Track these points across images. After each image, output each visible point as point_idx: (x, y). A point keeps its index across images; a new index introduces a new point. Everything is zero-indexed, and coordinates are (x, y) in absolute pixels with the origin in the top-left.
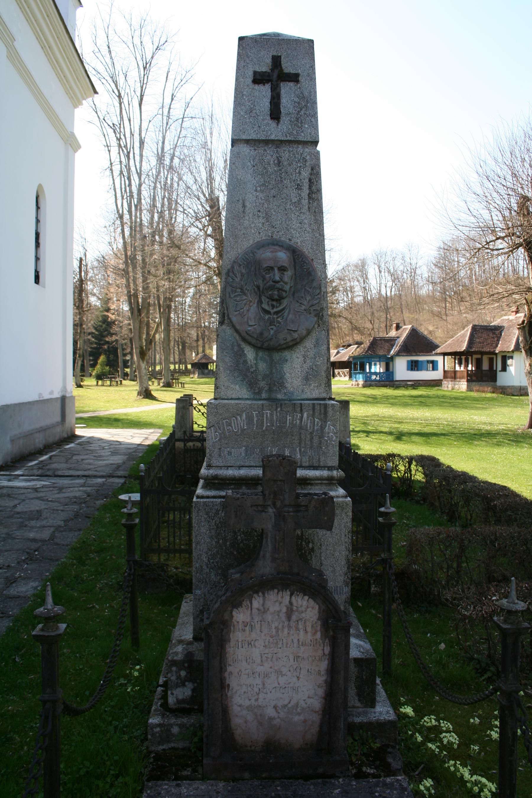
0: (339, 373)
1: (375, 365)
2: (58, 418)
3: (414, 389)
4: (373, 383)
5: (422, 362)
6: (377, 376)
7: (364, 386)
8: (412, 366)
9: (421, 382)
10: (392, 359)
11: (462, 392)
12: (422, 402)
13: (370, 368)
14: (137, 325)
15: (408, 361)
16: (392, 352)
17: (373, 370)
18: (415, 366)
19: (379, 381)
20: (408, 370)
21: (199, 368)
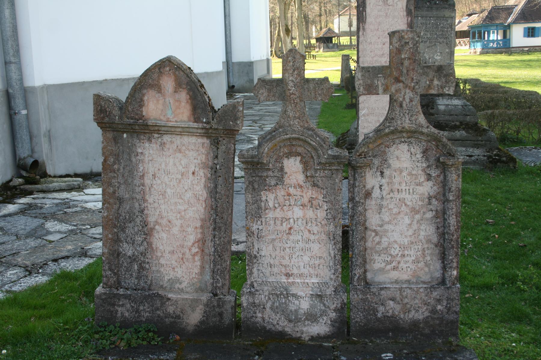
0: (460, 42)
1: (493, 33)
2: (266, 72)
3: (528, 54)
4: (490, 50)
5: (539, 28)
6: (493, 44)
7: (482, 53)
8: (529, 32)
9: (537, 48)
10: (509, 26)
12: (528, 64)
13: (489, 36)
14: (283, 7)
15: (525, 28)
16: (509, 20)
17: (491, 38)
18: (532, 32)
19: (496, 48)
20: (524, 36)
21: (324, 43)
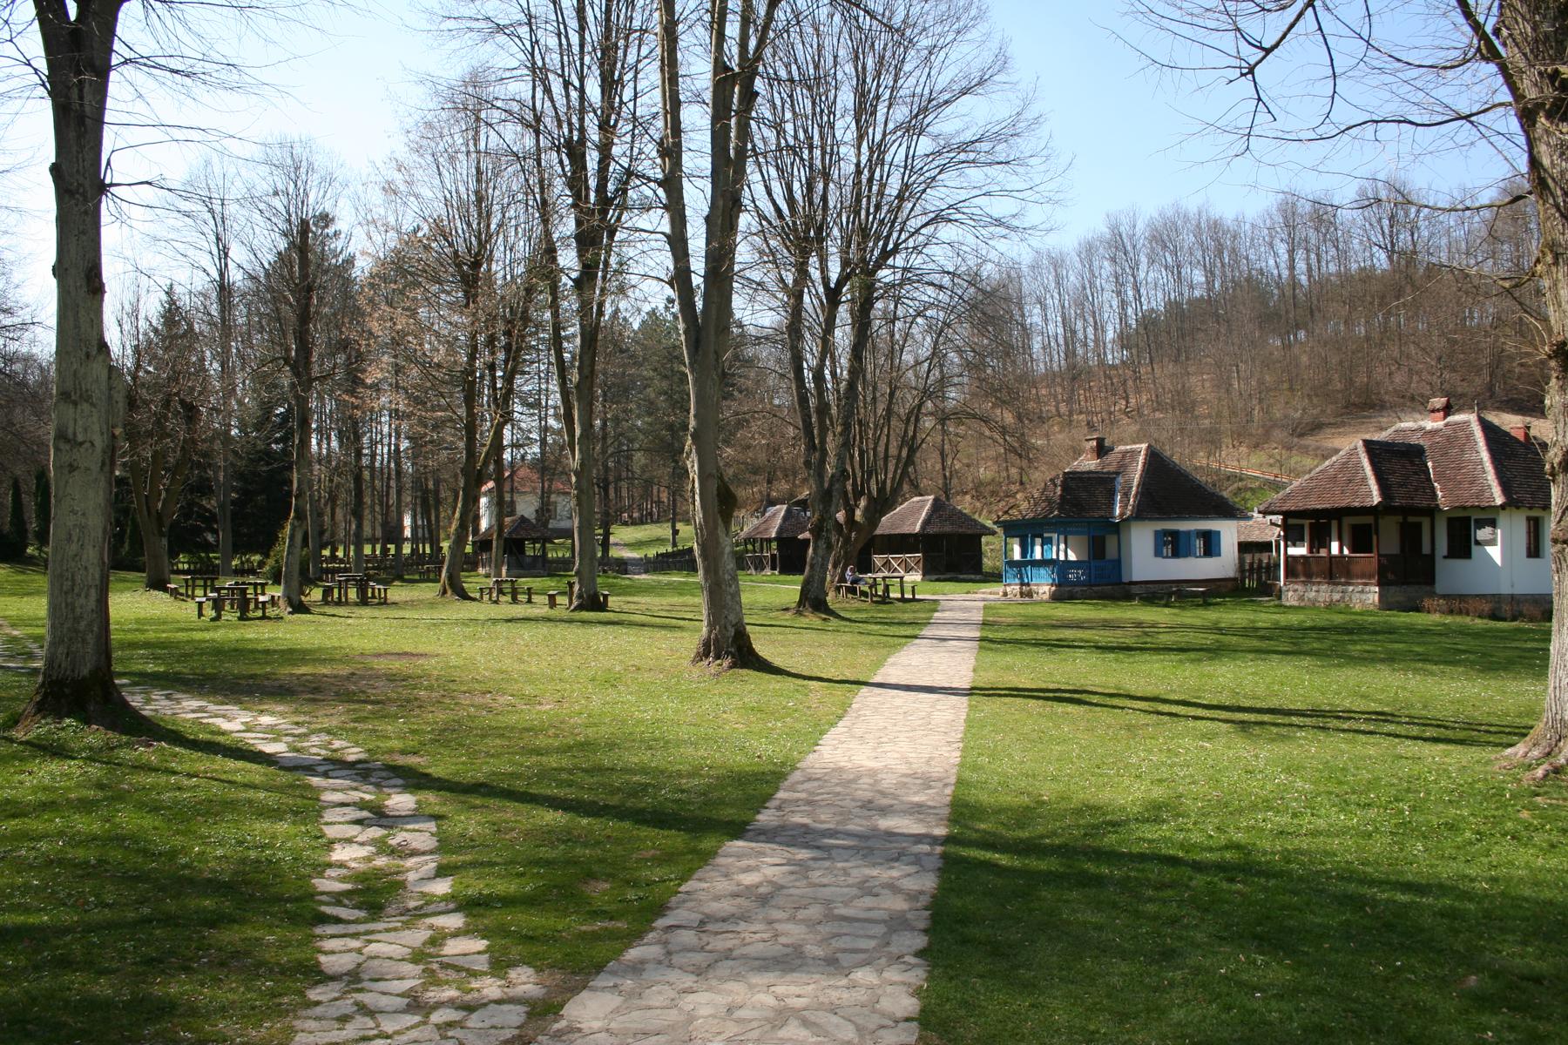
4: (1078, 589)
5: (1188, 533)
10: (1116, 529)
11: (1370, 613)
15: (1156, 533)
